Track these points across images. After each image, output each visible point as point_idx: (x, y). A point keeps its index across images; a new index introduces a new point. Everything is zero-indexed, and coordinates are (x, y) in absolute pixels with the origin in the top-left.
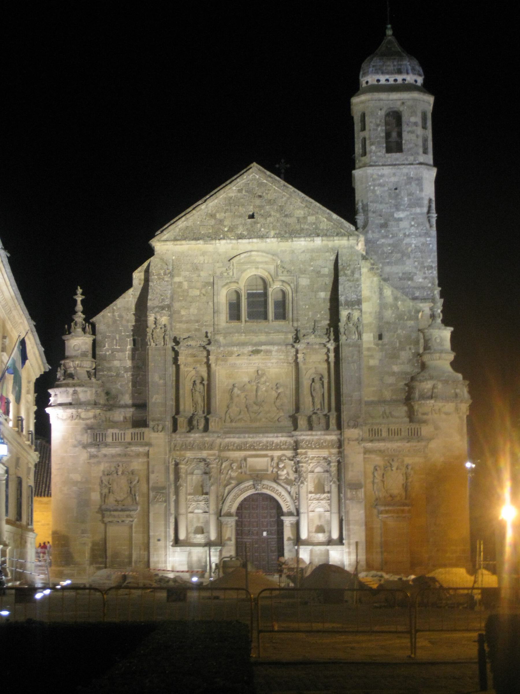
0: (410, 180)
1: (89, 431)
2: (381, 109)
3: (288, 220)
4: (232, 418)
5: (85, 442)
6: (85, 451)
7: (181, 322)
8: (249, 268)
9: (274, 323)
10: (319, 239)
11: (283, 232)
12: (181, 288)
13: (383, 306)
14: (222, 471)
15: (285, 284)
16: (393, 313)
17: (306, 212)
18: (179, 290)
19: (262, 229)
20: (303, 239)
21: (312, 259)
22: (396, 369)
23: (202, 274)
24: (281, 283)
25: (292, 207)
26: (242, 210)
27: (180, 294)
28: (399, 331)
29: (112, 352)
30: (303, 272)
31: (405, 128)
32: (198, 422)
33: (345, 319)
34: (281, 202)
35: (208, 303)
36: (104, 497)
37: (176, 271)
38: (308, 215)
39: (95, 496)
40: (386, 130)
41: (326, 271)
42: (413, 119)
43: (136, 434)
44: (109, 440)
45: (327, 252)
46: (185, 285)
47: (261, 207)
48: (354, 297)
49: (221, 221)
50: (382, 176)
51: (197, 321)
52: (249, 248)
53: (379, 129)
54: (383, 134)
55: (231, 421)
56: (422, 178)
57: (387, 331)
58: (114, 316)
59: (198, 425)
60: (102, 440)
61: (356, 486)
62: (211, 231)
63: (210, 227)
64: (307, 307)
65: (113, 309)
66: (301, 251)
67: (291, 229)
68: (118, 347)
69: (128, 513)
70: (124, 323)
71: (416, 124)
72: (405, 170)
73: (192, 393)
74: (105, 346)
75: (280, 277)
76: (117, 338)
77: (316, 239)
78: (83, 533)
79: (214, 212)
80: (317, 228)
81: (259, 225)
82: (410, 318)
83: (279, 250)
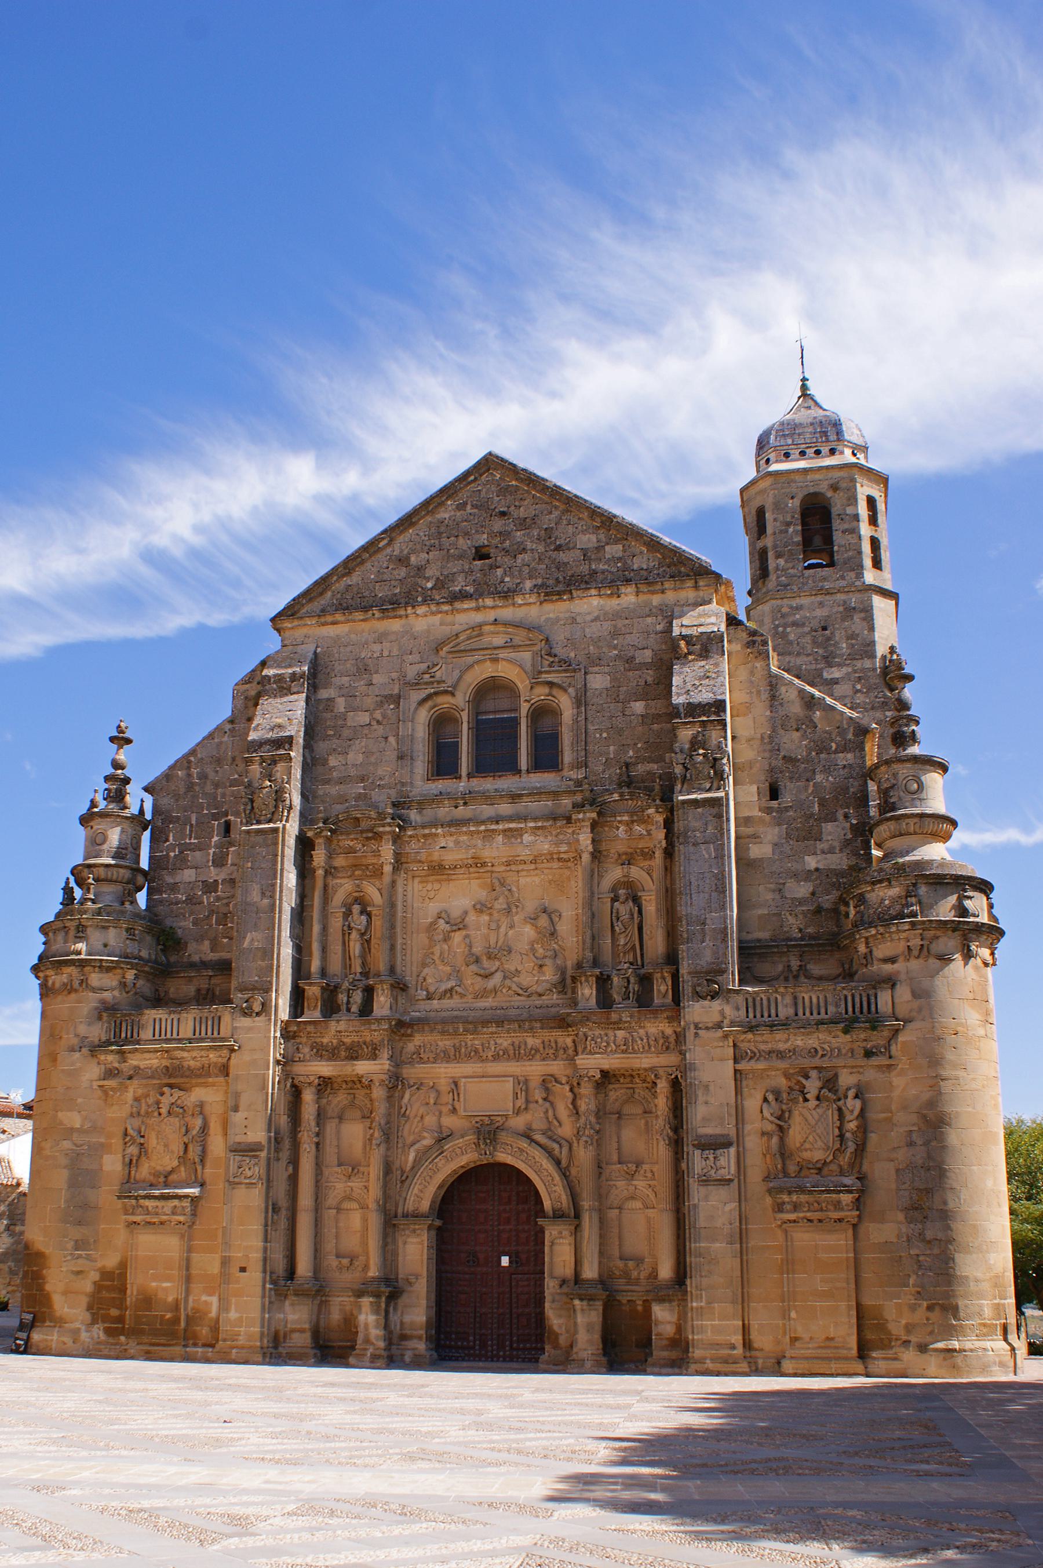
0: (849, 611)
1: (105, 1014)
2: (792, 498)
3: (563, 557)
4: (432, 989)
5: (97, 1042)
6: (95, 1061)
7: (327, 782)
8: (478, 662)
9: (532, 775)
10: (630, 589)
11: (551, 582)
12: (332, 711)
13: (779, 723)
14: (403, 1109)
15: (555, 692)
16: (804, 736)
17: (602, 537)
18: (328, 715)
19: (507, 579)
20: (593, 592)
21: (615, 634)
22: (812, 862)
23: (377, 679)
24: (546, 690)
25: (570, 529)
26: (463, 543)
27: (328, 723)
28: (819, 778)
29: (181, 852)
30: (596, 661)
31: (836, 524)
32: (349, 997)
33: (687, 746)
34: (548, 521)
35: (386, 738)
36: (130, 1164)
37: (320, 676)
38: (608, 544)
39: (112, 1164)
40: (803, 530)
41: (647, 656)
42: (849, 510)
43: (204, 1020)
44: (147, 1034)
45: (649, 616)
46: (341, 704)
47: (504, 535)
48: (704, 696)
49: (420, 569)
50: (799, 608)
51: (362, 780)
52: (478, 617)
53: (791, 530)
54: (798, 539)
55: (429, 997)
56: (872, 606)
57: (791, 778)
58: (189, 775)
59: (348, 1002)
60: (132, 1037)
61: (715, 1145)
62: (397, 591)
63: (396, 583)
64: (605, 735)
65: (189, 762)
66: (589, 618)
67: (570, 573)
68: (193, 841)
69: (176, 1202)
70: (209, 788)
71: (856, 517)
72: (840, 597)
73: (344, 935)
74: (167, 840)
75: (543, 676)
76: (194, 822)
77: (623, 590)
78: (76, 1249)
79: (405, 552)
80: (626, 568)
81: (499, 572)
82: (843, 749)
83: (543, 619)
